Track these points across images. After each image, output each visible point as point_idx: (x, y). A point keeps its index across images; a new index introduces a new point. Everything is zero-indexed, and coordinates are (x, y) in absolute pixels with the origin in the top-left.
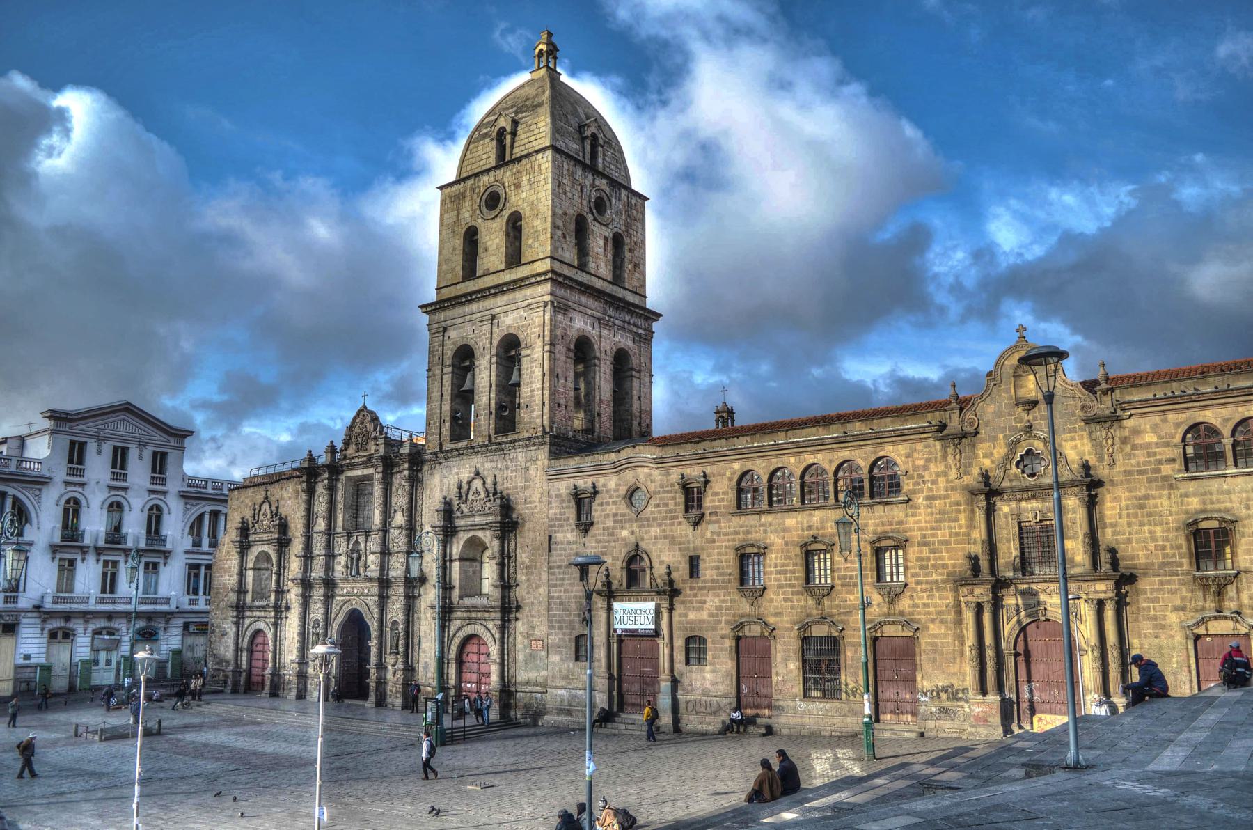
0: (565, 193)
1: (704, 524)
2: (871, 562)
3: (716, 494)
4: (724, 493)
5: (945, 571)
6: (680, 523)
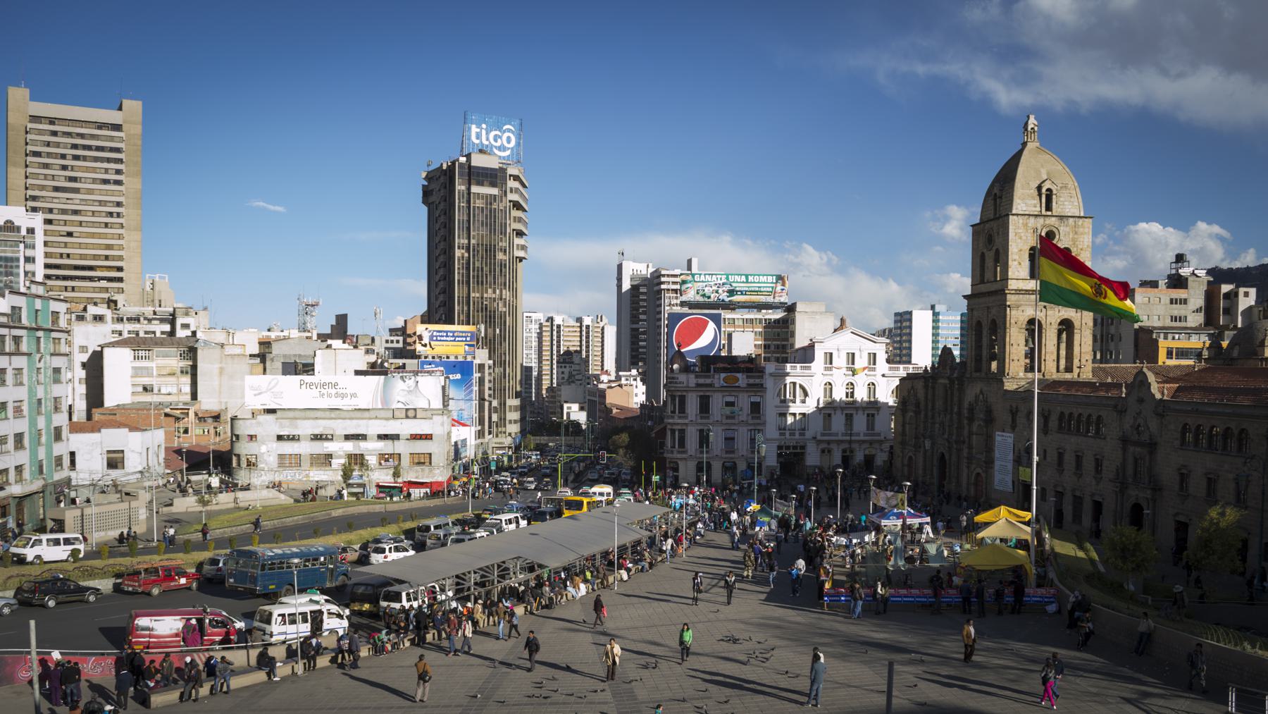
0: (1021, 238)
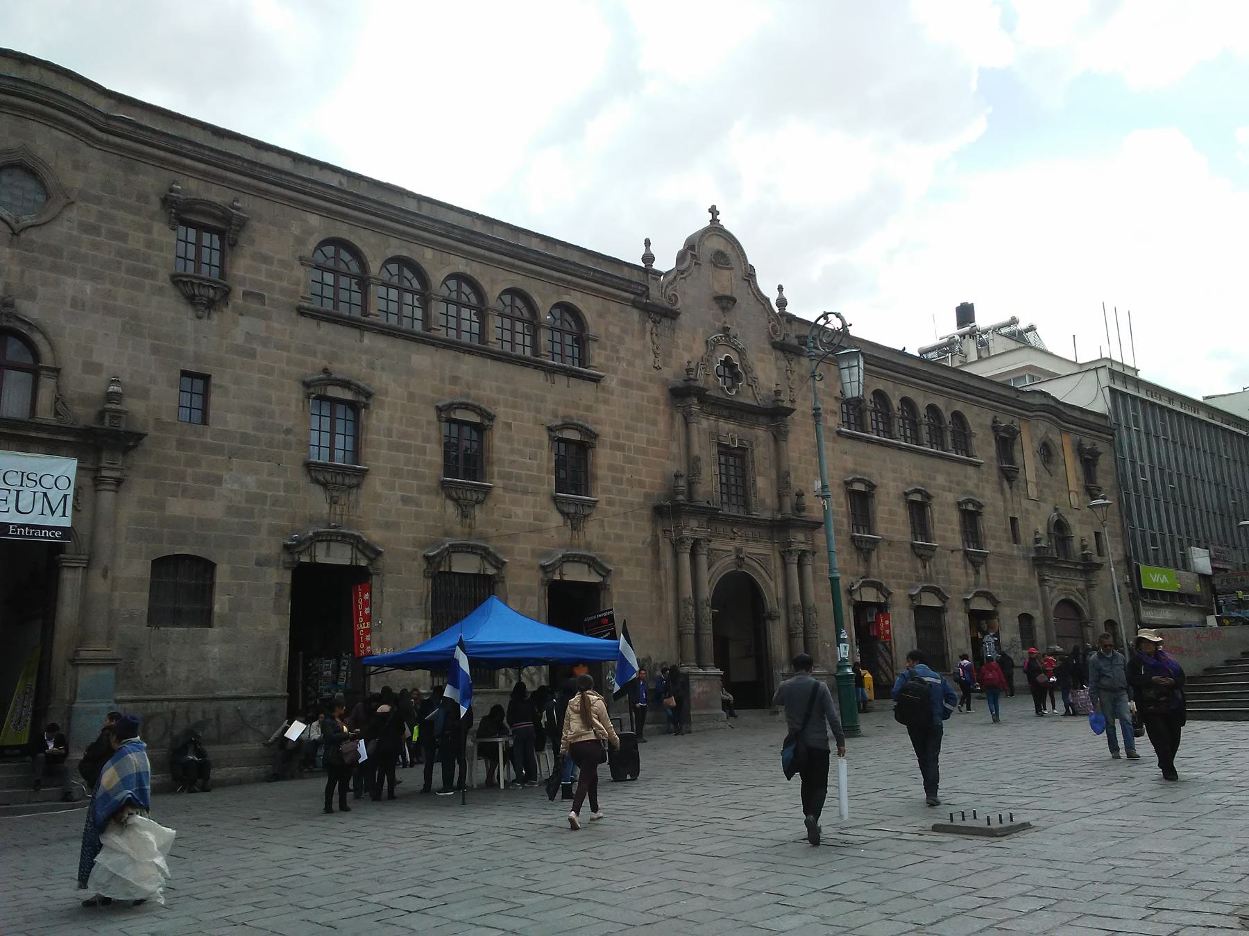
1: (228, 311)
2: (549, 460)
3: (266, 259)
4: (283, 263)
5: (643, 491)
6: (161, 291)
